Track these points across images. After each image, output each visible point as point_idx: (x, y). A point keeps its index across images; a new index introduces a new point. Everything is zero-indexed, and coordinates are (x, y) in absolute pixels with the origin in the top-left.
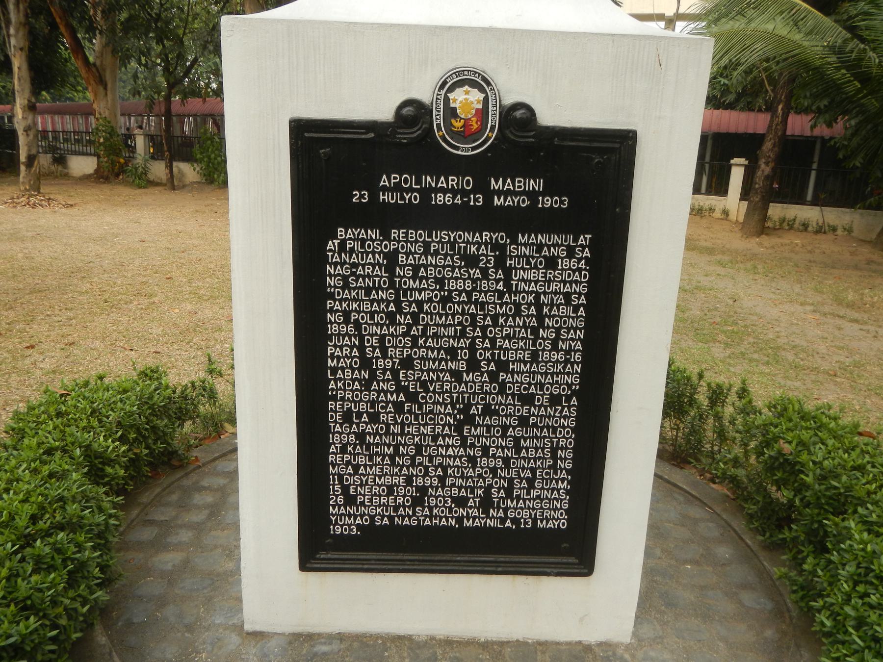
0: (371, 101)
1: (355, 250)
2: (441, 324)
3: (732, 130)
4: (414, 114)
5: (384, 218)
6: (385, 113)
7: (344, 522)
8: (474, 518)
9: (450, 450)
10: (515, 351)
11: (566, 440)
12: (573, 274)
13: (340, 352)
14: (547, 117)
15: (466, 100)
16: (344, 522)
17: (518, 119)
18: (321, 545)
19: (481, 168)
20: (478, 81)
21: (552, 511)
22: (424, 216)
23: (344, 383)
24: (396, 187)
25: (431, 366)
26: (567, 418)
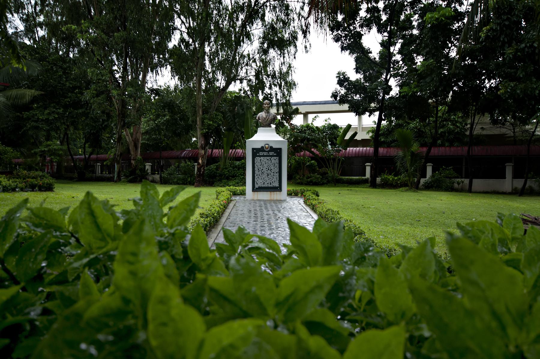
0: (259, 146)
1: (257, 159)
2: (265, 166)
3: (275, 193)
4: (262, 147)
5: (260, 156)
6: (260, 147)
7: (257, 186)
8: (269, 186)
9: (267, 178)
10: (272, 168)
11: (278, 177)
12: (277, 161)
13: (256, 169)
14: (274, 147)
15: (267, 146)
16: (257, 186)
17: (271, 147)
18: (254, 190)
19: (268, 152)
20: (268, 145)
21: (277, 184)
22: (264, 156)
23: (256, 172)
24: (261, 153)
25: (265, 169)
26: (278, 174)
